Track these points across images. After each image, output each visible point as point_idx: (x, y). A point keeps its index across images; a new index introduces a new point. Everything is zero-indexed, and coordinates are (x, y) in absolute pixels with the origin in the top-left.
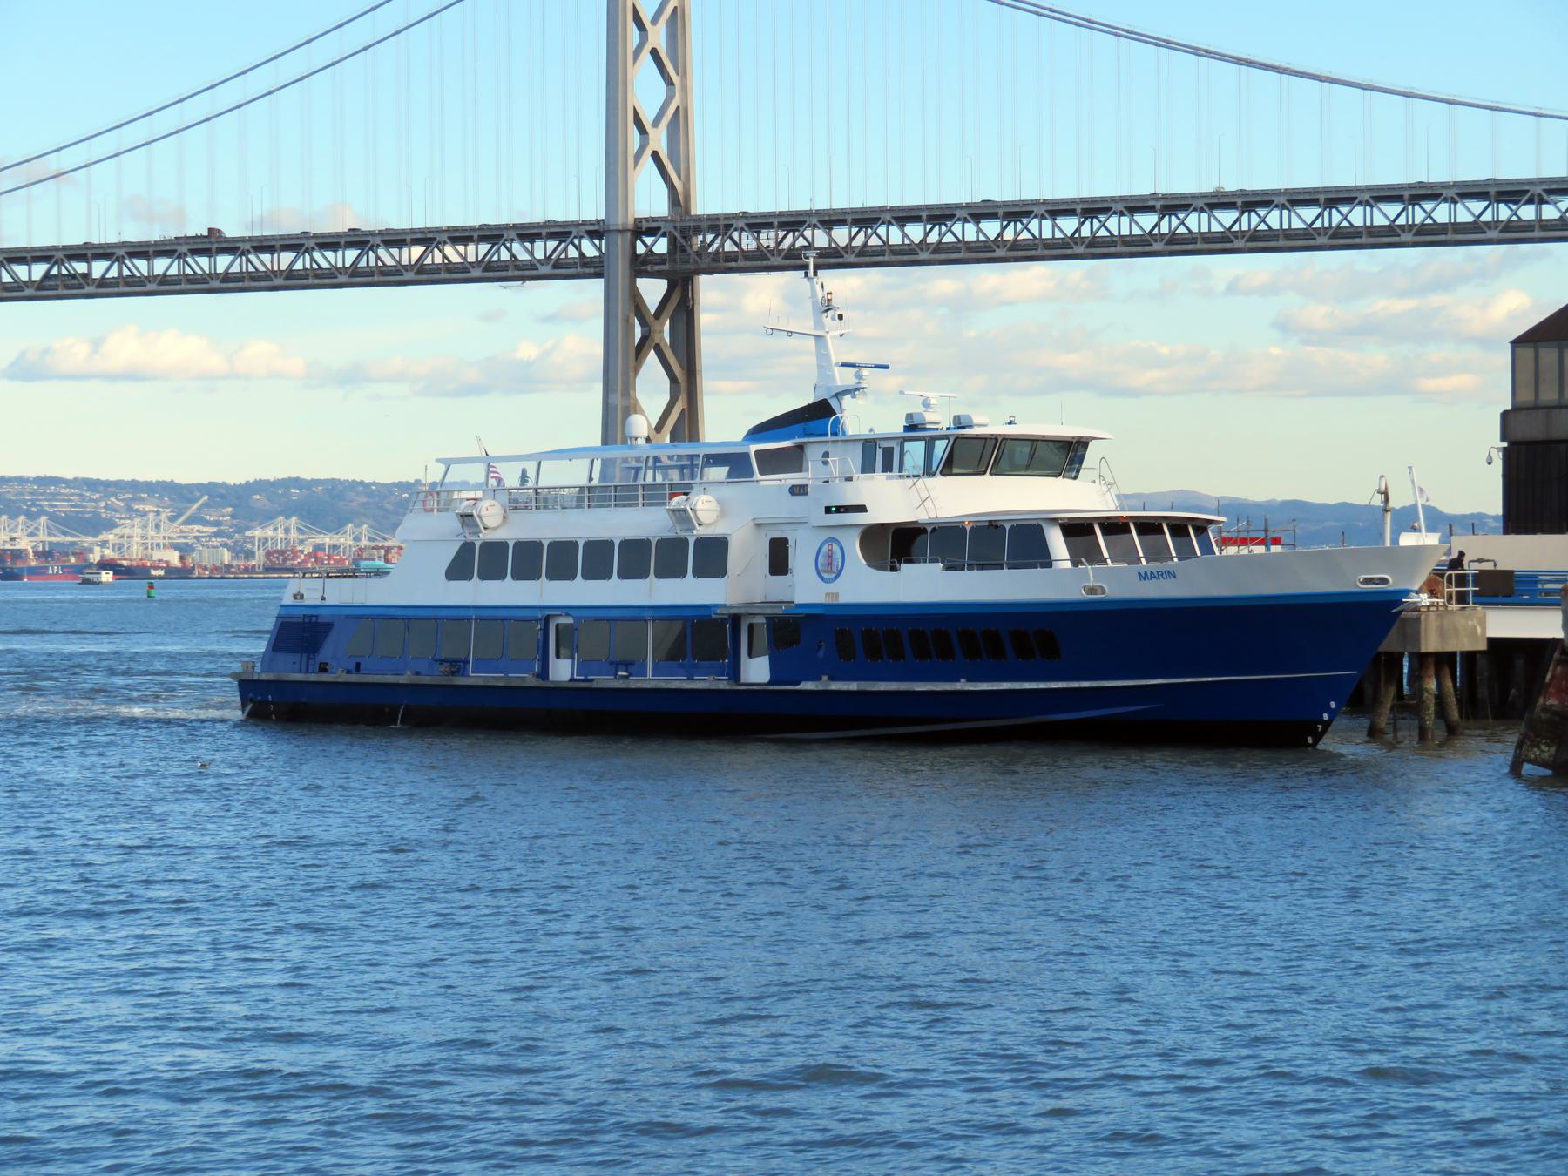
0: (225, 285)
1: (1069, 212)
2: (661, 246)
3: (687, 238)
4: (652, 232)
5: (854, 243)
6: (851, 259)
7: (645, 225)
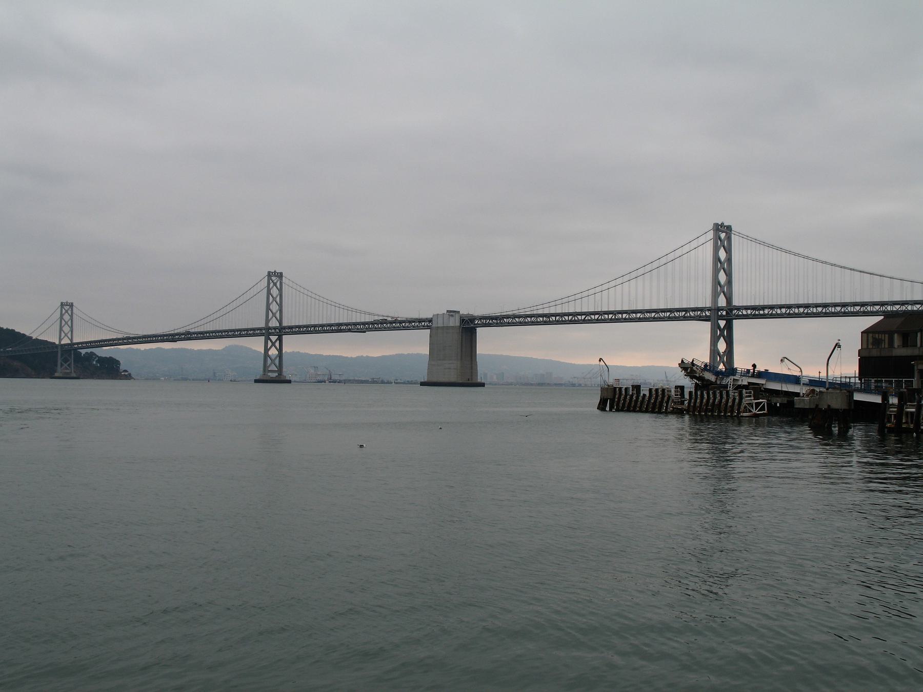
0: (864, 314)
1: (820, 306)
2: (724, 313)
3: (731, 312)
4: (722, 310)
5: (805, 312)
6: (768, 316)
7: (720, 308)
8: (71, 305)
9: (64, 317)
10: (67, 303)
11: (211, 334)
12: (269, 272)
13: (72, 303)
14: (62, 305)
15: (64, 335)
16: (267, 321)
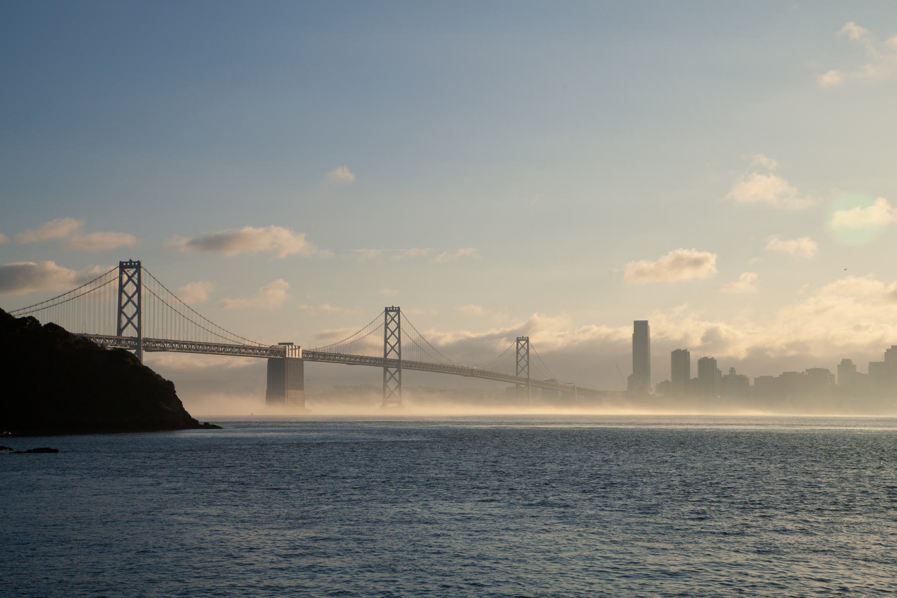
8: (398, 311)
9: (396, 326)
10: (393, 307)
11: (198, 347)
12: (121, 263)
13: (399, 308)
14: (387, 311)
15: (395, 348)
16: (120, 330)
